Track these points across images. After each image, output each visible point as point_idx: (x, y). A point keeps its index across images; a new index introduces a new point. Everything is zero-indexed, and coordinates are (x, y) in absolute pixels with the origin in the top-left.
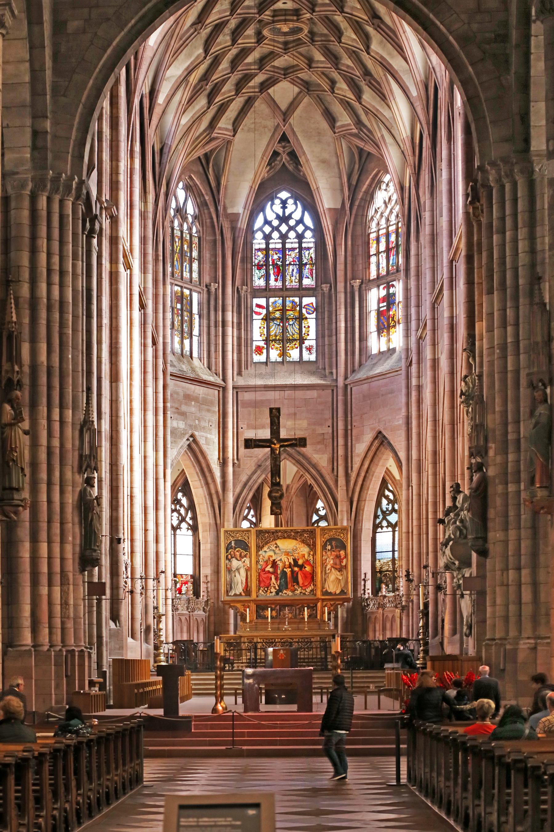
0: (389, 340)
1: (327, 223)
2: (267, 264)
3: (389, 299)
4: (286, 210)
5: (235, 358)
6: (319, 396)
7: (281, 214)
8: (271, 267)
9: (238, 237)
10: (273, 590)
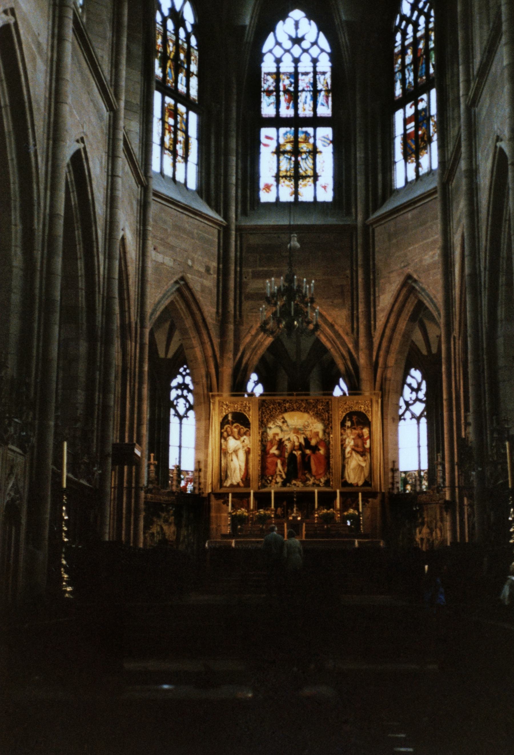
5: (239, 194)
8: (281, 93)
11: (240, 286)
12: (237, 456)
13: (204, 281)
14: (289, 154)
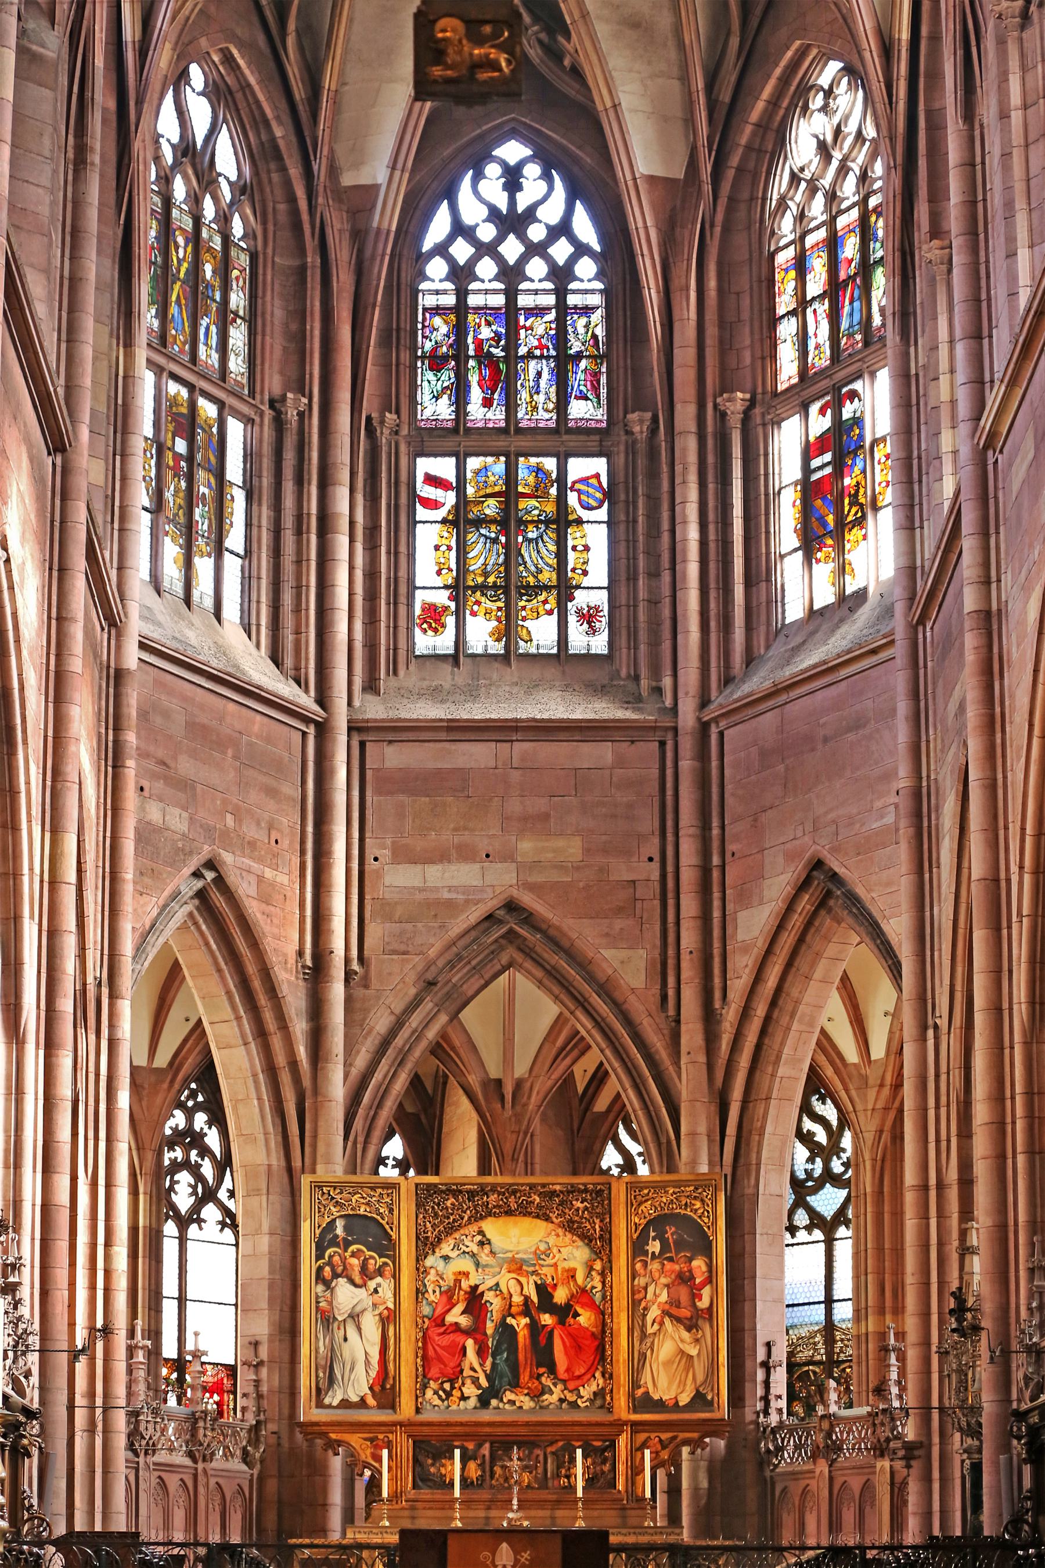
0: (842, 570)
1: (643, 220)
3: (842, 442)
4: (518, 195)
6: (620, 762)
7: (503, 206)
8: (472, 363)
9: (373, 257)
10: (470, 1390)
12: (359, 1329)
13: (267, 870)
14: (493, 528)
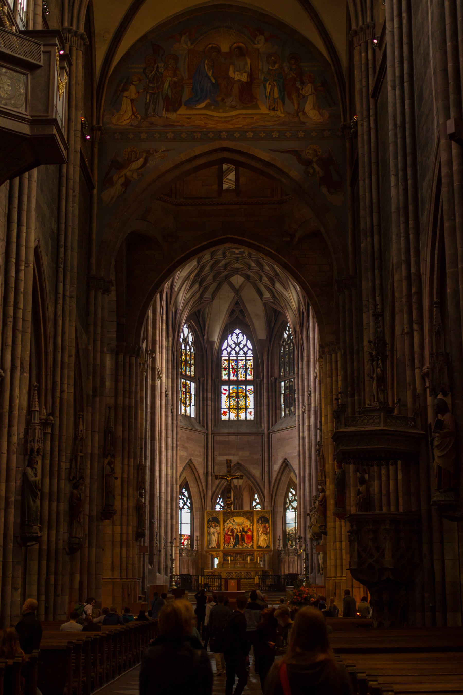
2: (229, 368)
8: (231, 369)
10: (232, 545)
11: (213, 459)
